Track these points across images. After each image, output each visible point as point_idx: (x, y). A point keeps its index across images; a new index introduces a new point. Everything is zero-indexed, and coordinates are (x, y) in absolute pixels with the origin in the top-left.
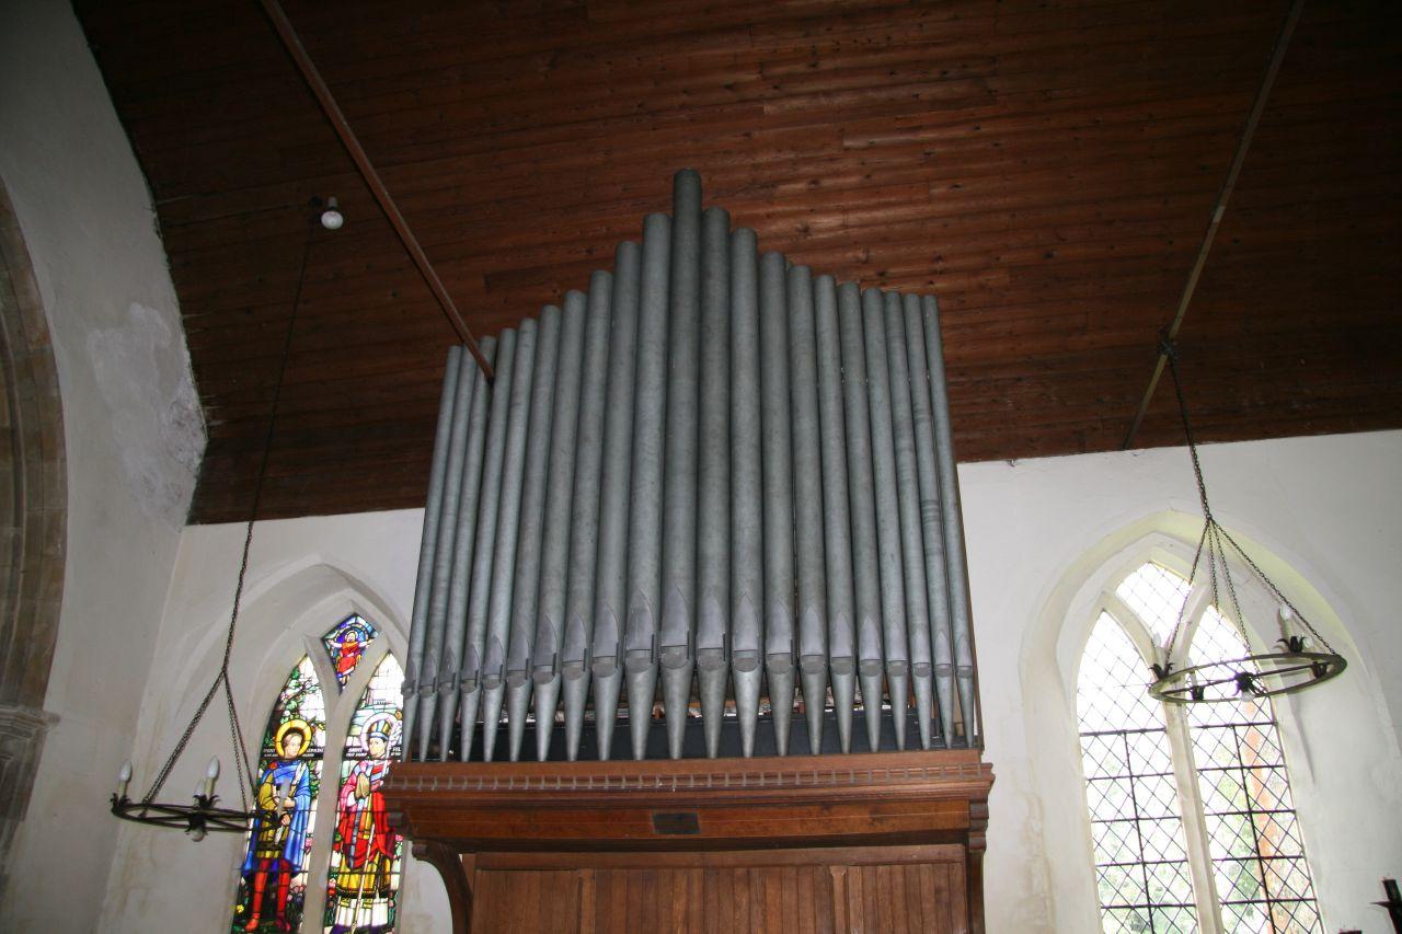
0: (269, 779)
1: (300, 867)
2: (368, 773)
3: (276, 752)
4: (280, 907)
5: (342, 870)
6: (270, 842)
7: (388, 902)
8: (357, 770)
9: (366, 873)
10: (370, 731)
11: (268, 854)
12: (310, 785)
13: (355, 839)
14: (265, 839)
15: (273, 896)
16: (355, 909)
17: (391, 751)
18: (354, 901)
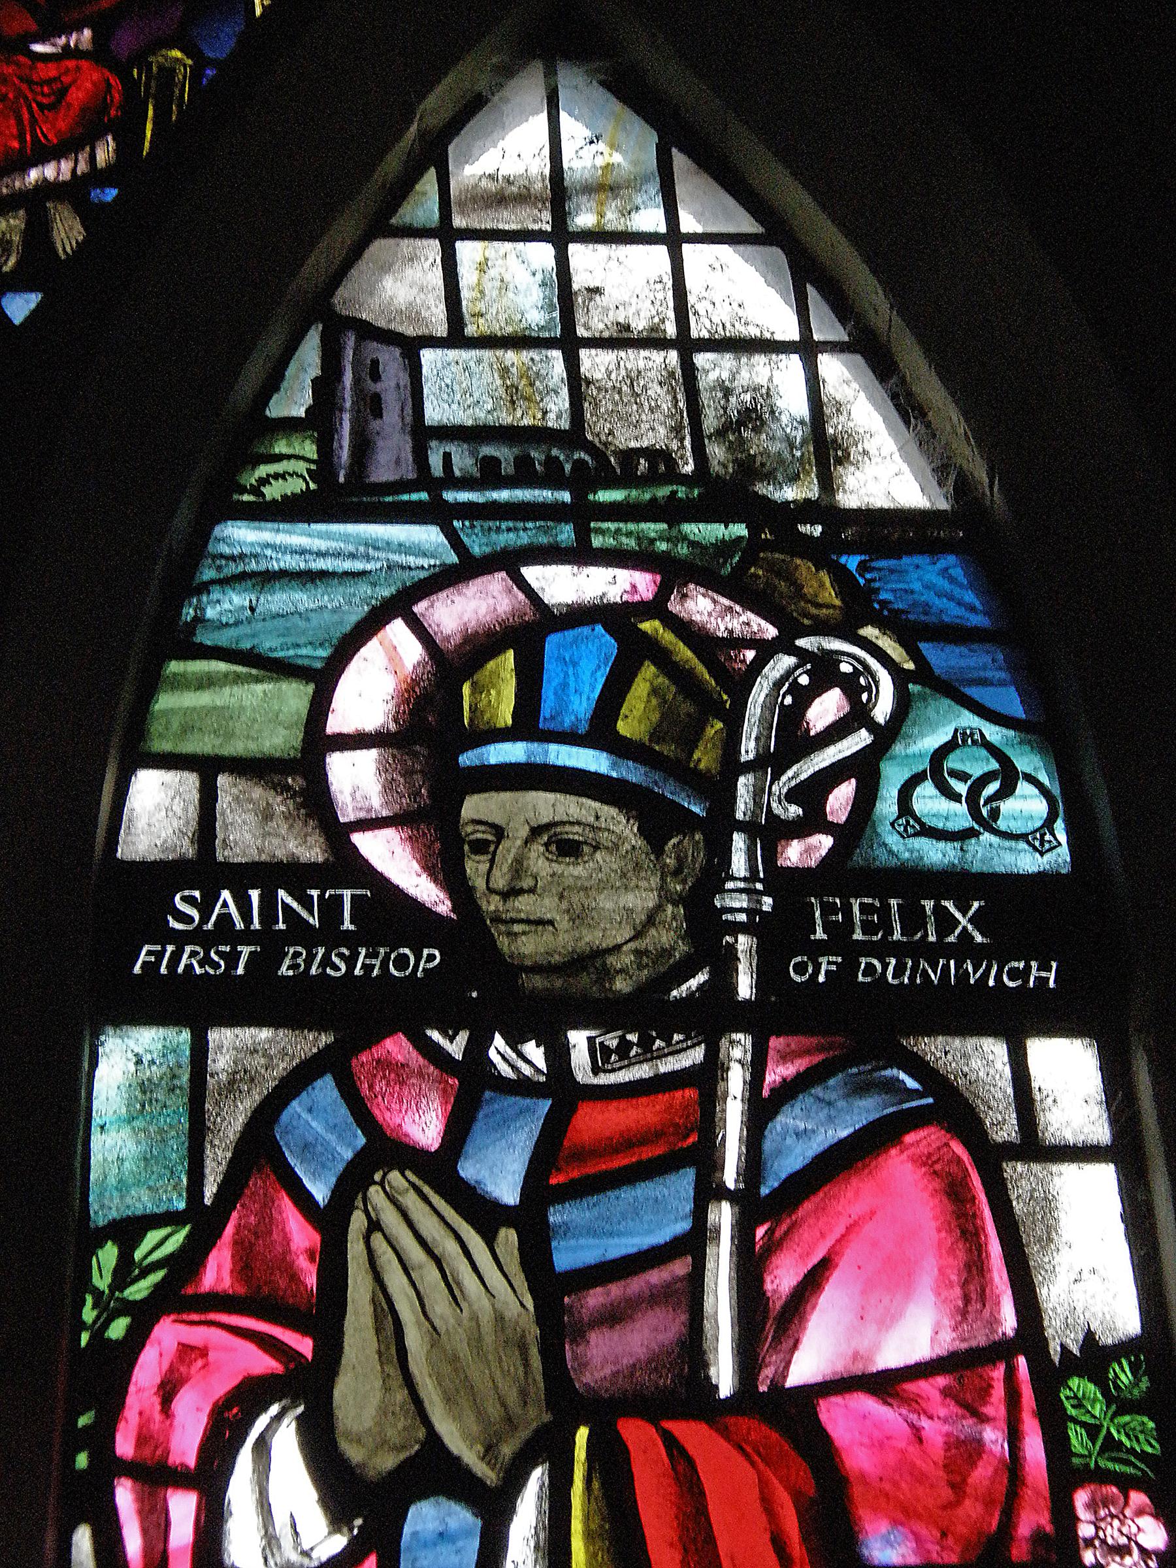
8: (320, 1132)
10: (428, 732)
17: (779, 937)
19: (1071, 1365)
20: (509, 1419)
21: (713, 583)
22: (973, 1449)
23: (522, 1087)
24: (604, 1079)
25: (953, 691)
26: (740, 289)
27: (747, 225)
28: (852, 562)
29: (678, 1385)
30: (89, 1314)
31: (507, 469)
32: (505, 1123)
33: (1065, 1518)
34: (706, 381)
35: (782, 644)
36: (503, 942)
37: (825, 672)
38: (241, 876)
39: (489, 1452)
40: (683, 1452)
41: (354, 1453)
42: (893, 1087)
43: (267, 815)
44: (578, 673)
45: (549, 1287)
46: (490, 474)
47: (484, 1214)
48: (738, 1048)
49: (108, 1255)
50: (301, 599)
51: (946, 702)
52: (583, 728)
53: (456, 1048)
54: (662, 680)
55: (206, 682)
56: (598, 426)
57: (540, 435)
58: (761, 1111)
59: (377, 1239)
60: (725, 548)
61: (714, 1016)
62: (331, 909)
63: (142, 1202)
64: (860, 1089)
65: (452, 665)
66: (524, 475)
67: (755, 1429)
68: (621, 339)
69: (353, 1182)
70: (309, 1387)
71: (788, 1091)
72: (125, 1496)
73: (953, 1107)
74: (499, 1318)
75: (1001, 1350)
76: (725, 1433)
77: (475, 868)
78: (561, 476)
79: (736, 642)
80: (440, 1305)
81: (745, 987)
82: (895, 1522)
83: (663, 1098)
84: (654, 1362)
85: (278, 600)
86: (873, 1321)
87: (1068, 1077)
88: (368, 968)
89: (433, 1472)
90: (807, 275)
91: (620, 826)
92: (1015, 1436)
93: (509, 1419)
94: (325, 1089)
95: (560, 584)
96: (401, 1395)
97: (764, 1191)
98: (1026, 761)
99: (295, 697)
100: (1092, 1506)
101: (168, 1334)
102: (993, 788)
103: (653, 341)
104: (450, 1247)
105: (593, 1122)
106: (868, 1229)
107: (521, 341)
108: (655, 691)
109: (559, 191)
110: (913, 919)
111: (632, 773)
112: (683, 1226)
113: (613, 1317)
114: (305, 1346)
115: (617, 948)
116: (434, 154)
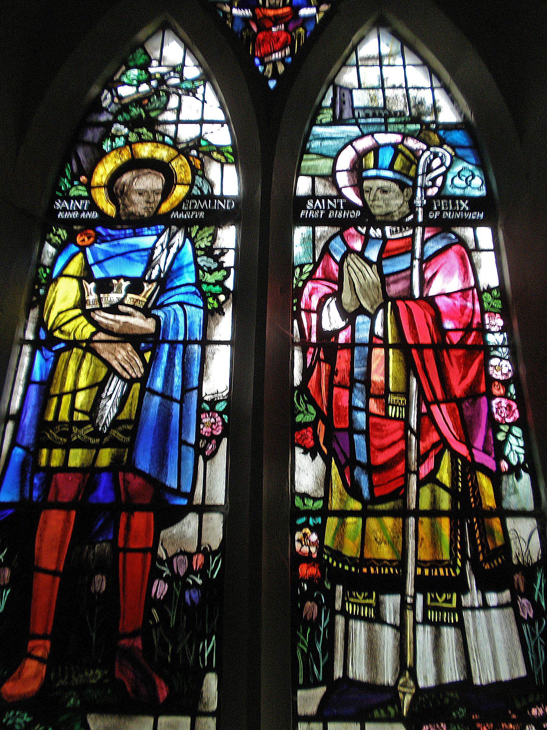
0: (75, 267)
1: (190, 496)
2: (373, 254)
3: (93, 206)
4: (130, 617)
5: (335, 504)
6: (81, 424)
7: (513, 604)
9: (418, 513)
10: (357, 169)
11: (76, 457)
12: (198, 283)
13: (361, 417)
14: (64, 415)
15: (100, 583)
16: (400, 629)
17: (427, 209)
18: (391, 602)
19: (484, 291)
20: (376, 302)
21: (413, 137)
22: (464, 307)
23: (377, 238)
24: (394, 237)
25: (463, 159)
26: (418, 76)
27: (419, 62)
28: (441, 133)
29: (408, 295)
30: (295, 281)
31: (371, 114)
32: (373, 245)
33: (483, 319)
34: (411, 96)
35: (428, 149)
36: (372, 211)
37: (436, 155)
38: (320, 198)
39: (372, 307)
40: (409, 307)
41: (346, 308)
42: (450, 238)
43: (325, 185)
44: (386, 156)
45: (383, 277)
46: (367, 116)
47: (370, 263)
48: (419, 230)
49: (298, 270)
50: (330, 143)
51: (460, 161)
52: (387, 168)
53: (363, 231)
54: (403, 158)
55: (312, 160)
56: (389, 106)
57: (377, 108)
58: (424, 243)
59: (349, 267)
60: (415, 131)
61: (414, 224)
62: (338, 205)
63: (304, 260)
64: (444, 238)
65: (361, 156)
66: (374, 116)
67: (423, 303)
68: (394, 87)
69: (344, 257)
70: (337, 295)
71: (429, 239)
72: (303, 314)
73: (462, 242)
74: (373, 282)
75: (472, 288)
76: (418, 304)
77: (366, 196)
78: (382, 116)
79: (418, 150)
80: (362, 280)
81: (420, 218)
82: (450, 320)
83: (404, 241)
84: (403, 291)
85: (326, 143)
86: (446, 282)
87: (485, 235)
88: (346, 216)
89: (361, 310)
90: (432, 72)
91: (395, 187)
92: (474, 304)
93: (376, 302)
94: (338, 239)
95: (382, 138)
96: (355, 297)
97: (424, 259)
98: (477, 173)
99: (330, 162)
100: (489, 317)
101: (310, 285)
102: (470, 178)
103: (400, 87)
104: (364, 269)
105: (390, 245)
106: (445, 265)
107: (373, 88)
108: (401, 160)
109: (380, 57)
110: (454, 205)
111: (398, 176)
112: (408, 265)
113: (395, 282)
114: (336, 287)
115: (395, 212)
116: (355, 49)
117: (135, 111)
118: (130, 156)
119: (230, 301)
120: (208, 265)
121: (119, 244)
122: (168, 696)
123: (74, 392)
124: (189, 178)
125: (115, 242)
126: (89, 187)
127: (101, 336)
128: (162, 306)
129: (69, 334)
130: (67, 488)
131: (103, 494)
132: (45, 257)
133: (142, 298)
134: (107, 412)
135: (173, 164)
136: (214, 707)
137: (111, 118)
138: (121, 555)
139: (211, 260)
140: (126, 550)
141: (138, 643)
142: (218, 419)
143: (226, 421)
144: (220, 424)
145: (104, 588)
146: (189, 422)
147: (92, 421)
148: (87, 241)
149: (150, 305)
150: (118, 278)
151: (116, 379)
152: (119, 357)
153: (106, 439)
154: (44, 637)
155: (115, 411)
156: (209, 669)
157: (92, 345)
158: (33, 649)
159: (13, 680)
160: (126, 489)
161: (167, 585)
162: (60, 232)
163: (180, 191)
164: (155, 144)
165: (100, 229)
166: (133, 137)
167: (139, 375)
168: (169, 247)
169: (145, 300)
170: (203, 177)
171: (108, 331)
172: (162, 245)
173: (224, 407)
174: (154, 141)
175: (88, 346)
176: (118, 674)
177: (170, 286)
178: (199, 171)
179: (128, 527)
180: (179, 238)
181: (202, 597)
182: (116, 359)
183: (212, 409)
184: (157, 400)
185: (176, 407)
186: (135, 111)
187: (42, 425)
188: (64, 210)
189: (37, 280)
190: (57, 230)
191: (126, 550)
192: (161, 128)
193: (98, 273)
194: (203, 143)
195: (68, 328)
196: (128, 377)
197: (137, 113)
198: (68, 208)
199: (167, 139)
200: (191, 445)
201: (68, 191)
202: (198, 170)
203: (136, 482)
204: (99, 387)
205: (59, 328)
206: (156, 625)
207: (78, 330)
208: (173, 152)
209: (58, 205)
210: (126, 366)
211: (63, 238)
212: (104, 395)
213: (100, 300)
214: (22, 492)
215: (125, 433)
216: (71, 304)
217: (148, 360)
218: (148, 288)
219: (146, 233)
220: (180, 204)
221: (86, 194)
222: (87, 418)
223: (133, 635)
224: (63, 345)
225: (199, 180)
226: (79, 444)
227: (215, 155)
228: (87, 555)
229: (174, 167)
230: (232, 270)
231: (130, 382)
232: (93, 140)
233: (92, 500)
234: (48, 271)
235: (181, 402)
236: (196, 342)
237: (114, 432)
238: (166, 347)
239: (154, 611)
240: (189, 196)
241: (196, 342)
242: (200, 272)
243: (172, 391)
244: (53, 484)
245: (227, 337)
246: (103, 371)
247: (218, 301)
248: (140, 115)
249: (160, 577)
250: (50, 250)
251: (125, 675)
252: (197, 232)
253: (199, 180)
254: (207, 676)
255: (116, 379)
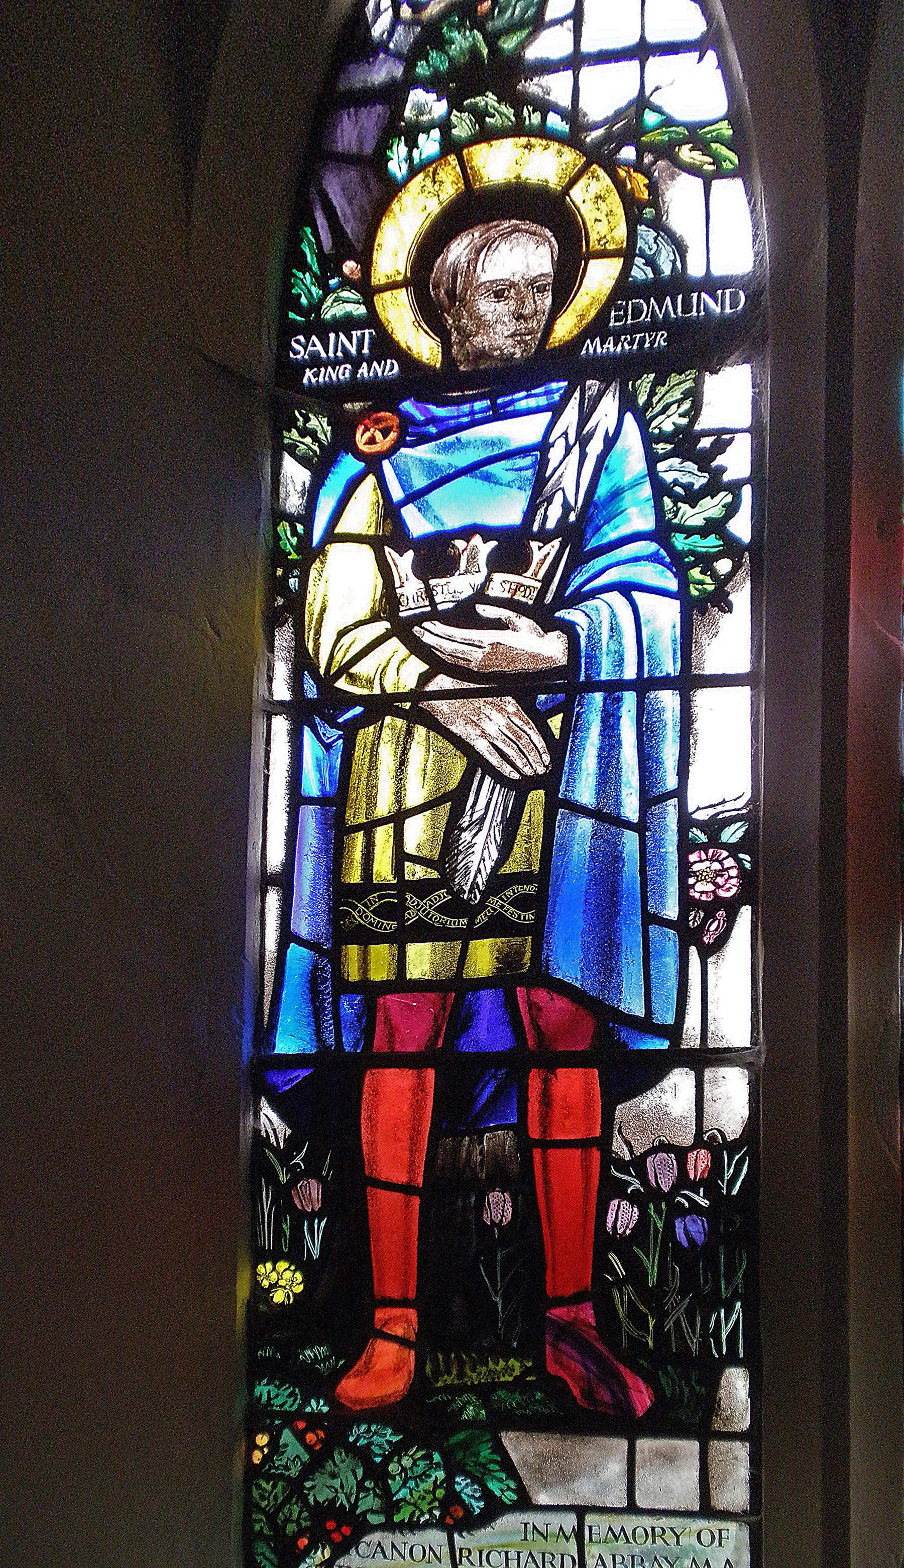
0: (361, 514)
1: (675, 1032)
3: (385, 345)
6: (423, 888)
11: (421, 960)
12: (663, 531)
15: (500, 1207)
117: (461, 41)
118: (461, 185)
119: (744, 572)
120: (685, 479)
121: (459, 440)
122: (653, 1404)
123: (398, 818)
124: (621, 232)
125: (451, 438)
126: (367, 290)
127: (443, 682)
128: (579, 598)
129: (370, 682)
130: (413, 1027)
131: (487, 1034)
132: (288, 495)
133: (530, 580)
134: (476, 858)
135: (577, 194)
136: (744, 1423)
137: (399, 71)
138: (537, 1154)
139: (691, 466)
140: (546, 1144)
141: (588, 1313)
142: (730, 862)
143: (748, 866)
144: (734, 873)
145: (509, 1216)
146: (662, 874)
147: (446, 881)
148: (383, 443)
149: (549, 598)
150: (467, 533)
151: (488, 780)
152: (491, 728)
153: (482, 919)
154: (403, 1303)
155: (495, 855)
156: (732, 1360)
157: (423, 705)
158: (386, 1323)
159: (356, 1376)
160: (534, 1021)
161: (636, 1209)
162: (313, 423)
163: (600, 277)
164: (524, 140)
165: (407, 406)
166: (462, 128)
167: (541, 770)
168: (583, 440)
169: (539, 585)
170: (658, 225)
171: (456, 670)
172: (566, 434)
173: (740, 833)
174: (518, 130)
175: (415, 708)
176: (552, 1368)
177: (594, 543)
178: (643, 211)
179: (546, 1099)
180: (608, 409)
181: (711, 1232)
182: (484, 735)
183: (714, 841)
184: (585, 825)
185: (630, 840)
186: (461, 41)
187: (340, 895)
188: (316, 362)
189: (277, 556)
190: (307, 420)
191: (546, 1144)
192: (533, 87)
193: (417, 523)
194: (651, 118)
195: (362, 669)
196: (516, 776)
197: (466, 45)
198: (323, 355)
199: (554, 121)
200: (668, 923)
201: (316, 307)
202: (643, 205)
203: (556, 1007)
204: (453, 801)
205: (345, 669)
206: (619, 1283)
207: (388, 669)
208: (571, 157)
209: (299, 350)
210: (508, 751)
211: (323, 437)
212: (465, 821)
213: (429, 593)
214: (318, 1033)
215: (520, 903)
216: (364, 613)
217: (557, 733)
218: (542, 554)
219: (522, 405)
220: (603, 315)
221: (362, 310)
222: (435, 875)
223: (578, 1299)
224: (358, 710)
225: (646, 235)
226: (424, 932)
227: (686, 153)
228: (469, 1153)
229: (579, 203)
230: (747, 491)
231: (521, 788)
232: (361, 147)
233: (467, 1046)
234: (300, 528)
235: (641, 827)
236: (665, 683)
237: (494, 902)
238: (598, 697)
239: (612, 1257)
240: (624, 288)
241: (665, 683)
242: (667, 500)
243: (618, 804)
244: (380, 1016)
245: (743, 665)
246: (458, 766)
247: (714, 575)
248: (474, 51)
249: (623, 1196)
250: (295, 474)
251: (568, 1368)
252: (652, 393)
253: (646, 235)
254: (727, 1371)
255: (488, 780)
